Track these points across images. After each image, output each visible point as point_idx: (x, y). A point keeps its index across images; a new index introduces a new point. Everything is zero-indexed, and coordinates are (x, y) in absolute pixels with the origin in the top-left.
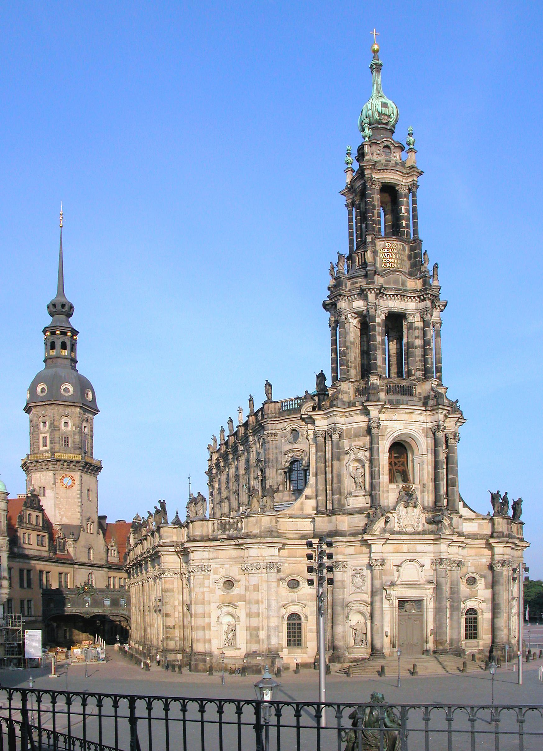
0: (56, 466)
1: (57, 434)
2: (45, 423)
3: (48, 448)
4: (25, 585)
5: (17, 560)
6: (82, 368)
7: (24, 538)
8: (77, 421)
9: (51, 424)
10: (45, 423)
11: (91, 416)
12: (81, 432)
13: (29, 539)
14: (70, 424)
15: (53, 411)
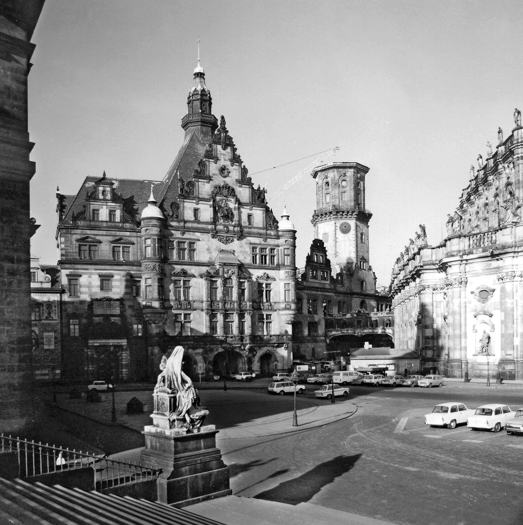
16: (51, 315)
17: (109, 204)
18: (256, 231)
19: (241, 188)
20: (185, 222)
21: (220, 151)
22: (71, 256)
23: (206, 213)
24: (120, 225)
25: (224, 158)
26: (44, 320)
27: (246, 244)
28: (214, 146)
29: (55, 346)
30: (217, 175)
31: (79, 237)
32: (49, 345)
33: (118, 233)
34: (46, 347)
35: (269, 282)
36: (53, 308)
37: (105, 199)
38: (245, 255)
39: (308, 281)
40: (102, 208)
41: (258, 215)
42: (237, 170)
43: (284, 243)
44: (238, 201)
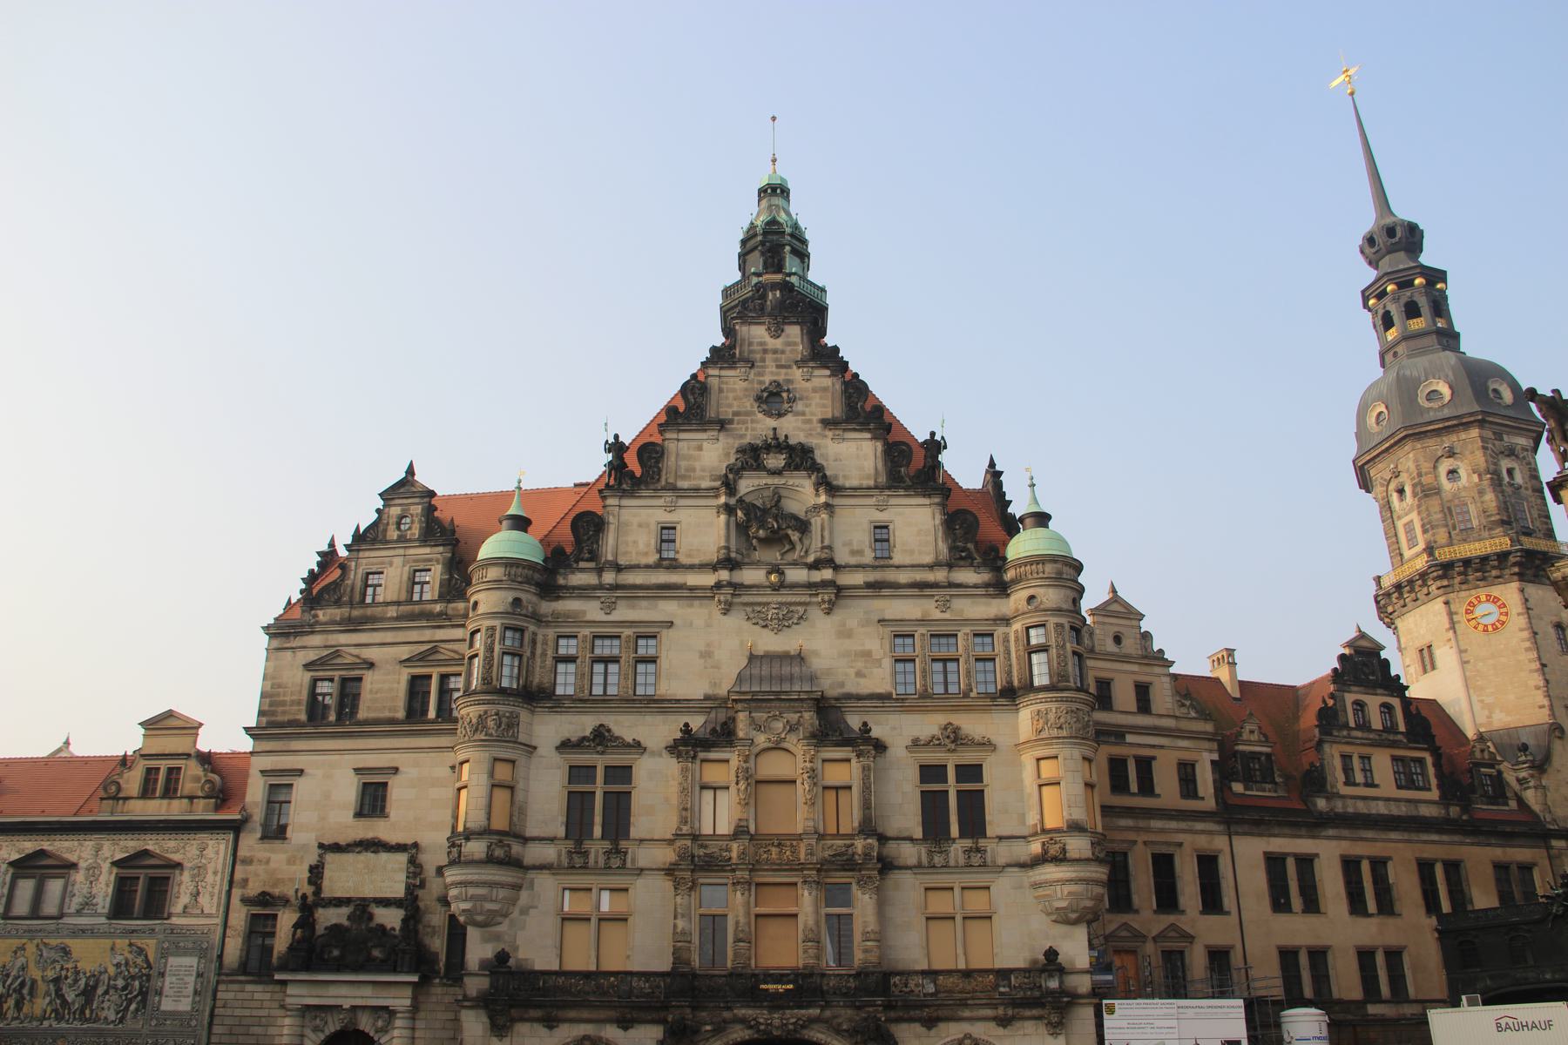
0: (1445, 583)
1: (1434, 504)
2: (1401, 491)
3: (1421, 546)
4: (1372, 906)
5: (1331, 832)
6: (1471, 347)
7: (1348, 770)
8: (1480, 459)
9: (1414, 486)
10: (1401, 491)
11: (1522, 441)
12: (1497, 482)
13: (1367, 771)
14: (1462, 472)
15: (1409, 460)
16: (200, 899)
17: (412, 551)
18: (903, 577)
19: (844, 445)
20: (619, 569)
21: (761, 344)
22: (284, 713)
23: (704, 530)
24: (438, 608)
25: (776, 360)
26: (178, 915)
27: (865, 623)
28: (743, 330)
29: (194, 1002)
30: (747, 414)
31: (312, 656)
32: (178, 996)
33: (428, 635)
34: (167, 1005)
35: (969, 757)
36: (210, 878)
37: (402, 539)
38: (860, 665)
39: (1332, 796)
40: (391, 564)
41: (916, 526)
42: (825, 389)
43: (1023, 606)
44: (826, 484)
